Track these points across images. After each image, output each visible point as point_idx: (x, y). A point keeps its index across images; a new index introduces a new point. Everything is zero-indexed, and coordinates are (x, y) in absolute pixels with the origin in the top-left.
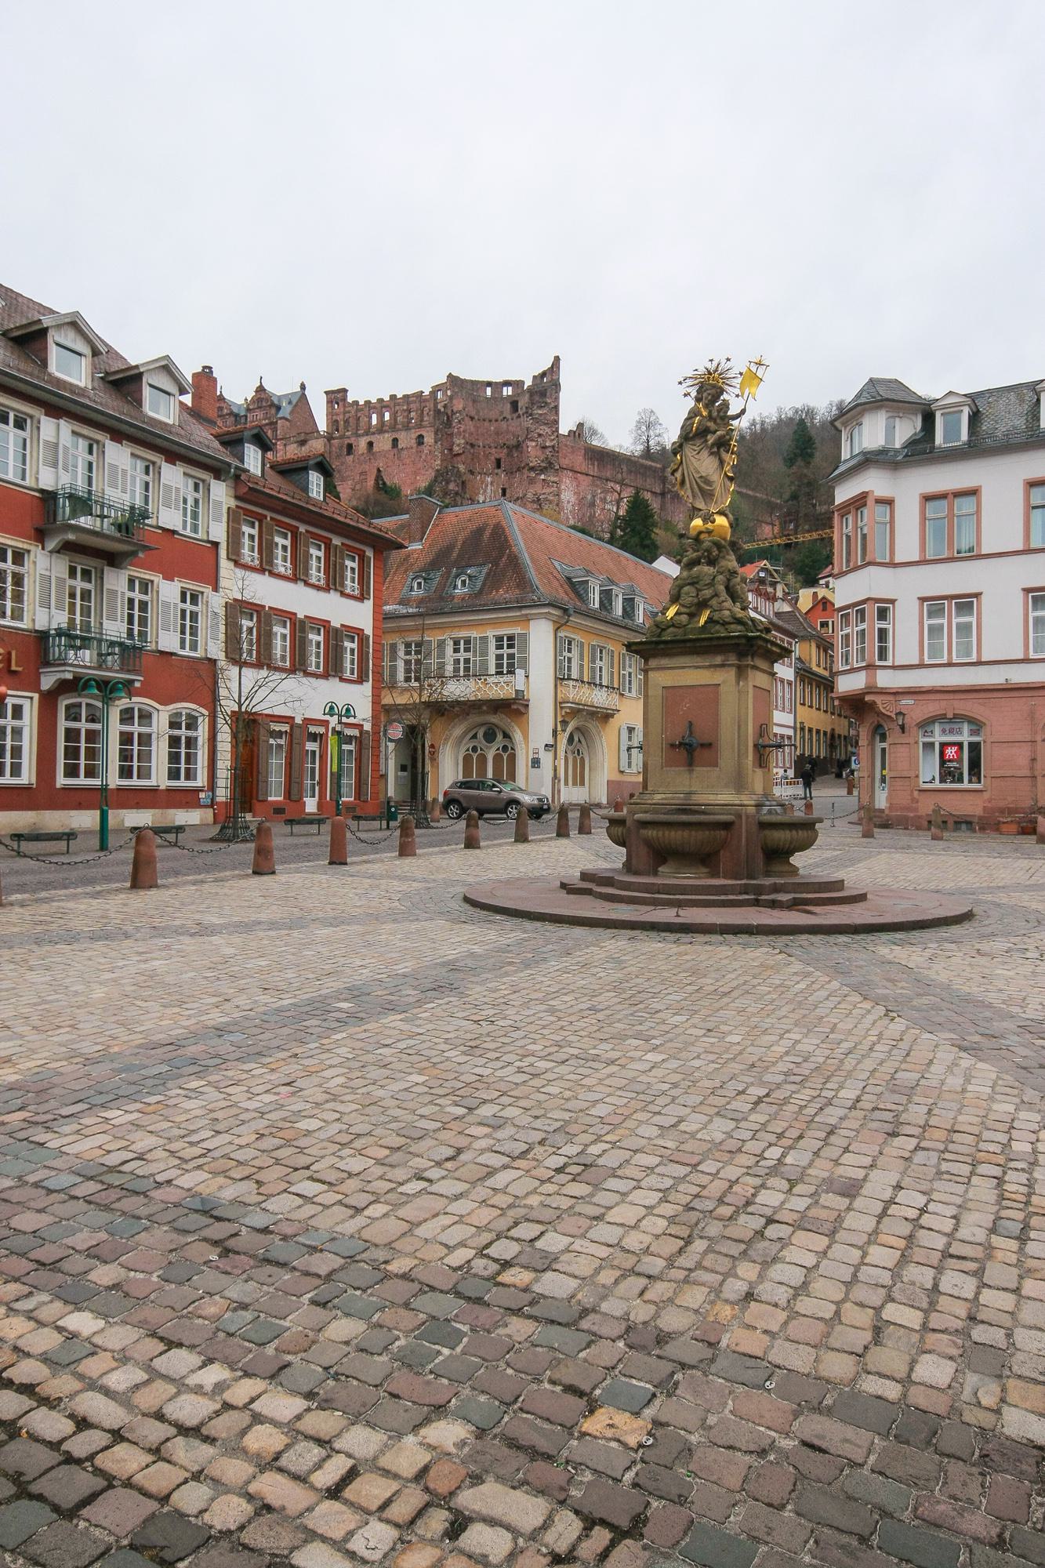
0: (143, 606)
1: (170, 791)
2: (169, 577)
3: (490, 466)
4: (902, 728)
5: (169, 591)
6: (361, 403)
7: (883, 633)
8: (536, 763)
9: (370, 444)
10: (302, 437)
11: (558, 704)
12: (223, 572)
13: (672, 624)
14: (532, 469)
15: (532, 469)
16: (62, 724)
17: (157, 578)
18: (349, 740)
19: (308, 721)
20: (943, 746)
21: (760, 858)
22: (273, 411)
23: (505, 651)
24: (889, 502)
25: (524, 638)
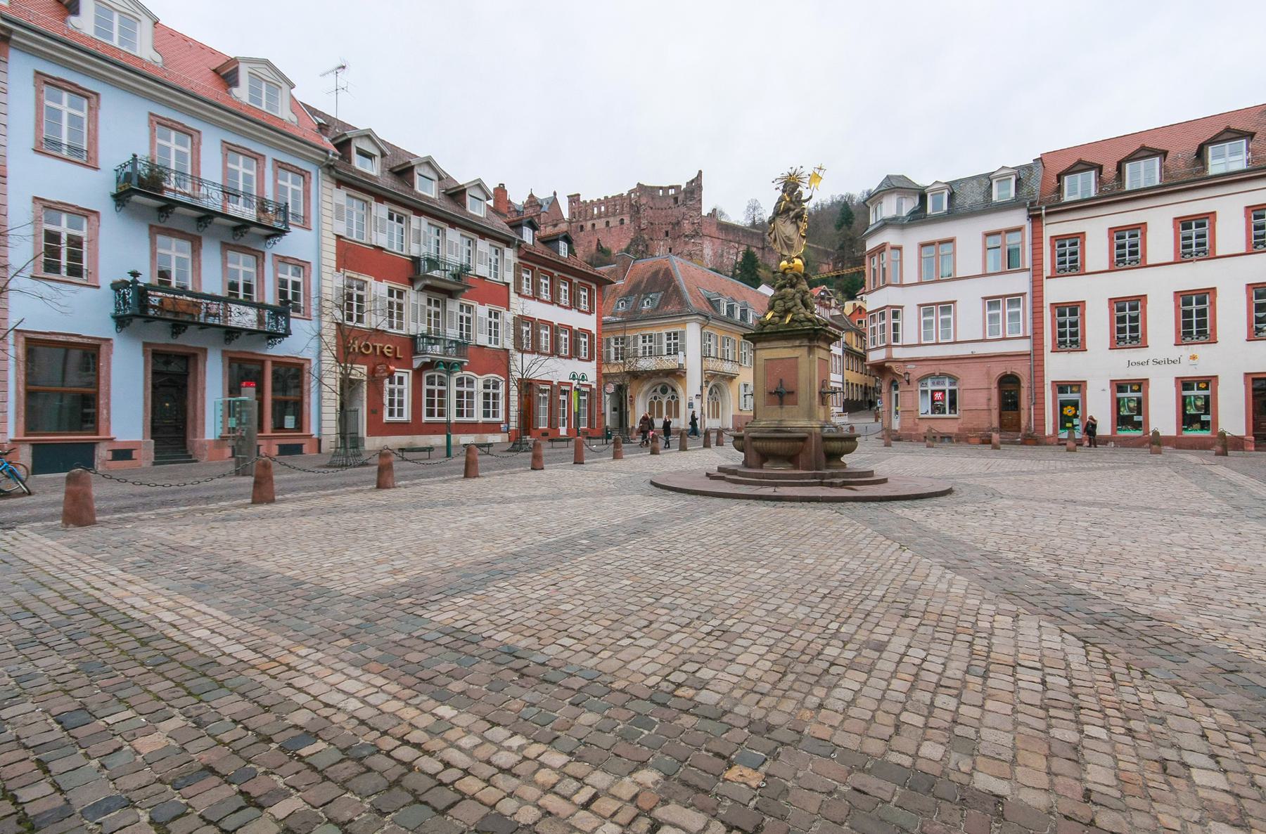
0: (468, 320)
1: (484, 423)
2: (482, 304)
3: (662, 235)
4: (908, 382)
5: (482, 311)
7: (896, 326)
8: (691, 405)
9: (594, 225)
11: (703, 371)
12: (512, 300)
13: (770, 322)
16: (425, 387)
17: (475, 304)
18: (584, 393)
19: (560, 383)
20: (933, 392)
23: (672, 341)
24: (900, 248)
25: (683, 333)
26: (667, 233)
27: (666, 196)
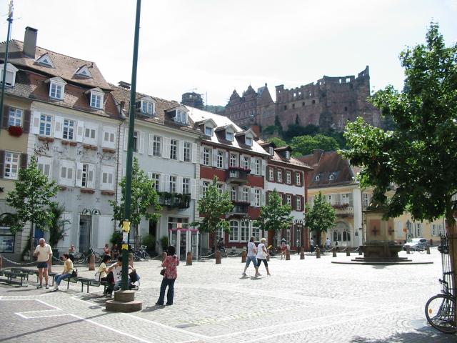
3: (342, 110)
5: (253, 190)
6: (289, 89)
8: (357, 234)
9: (294, 105)
10: (267, 104)
12: (265, 184)
14: (361, 110)
15: (361, 110)
17: (249, 187)
18: (298, 228)
26: (346, 109)
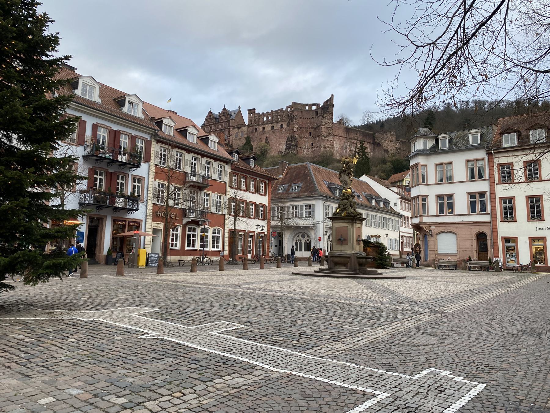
1: (212, 251)
3: (307, 135)
4: (432, 235)
6: (261, 113)
7: (424, 205)
9: (264, 128)
13: (338, 213)
14: (323, 136)
16: (187, 233)
17: (211, 193)
19: (249, 232)
21: (357, 265)
22: (229, 116)
24: (426, 166)
26: (310, 133)
27: (310, 110)
